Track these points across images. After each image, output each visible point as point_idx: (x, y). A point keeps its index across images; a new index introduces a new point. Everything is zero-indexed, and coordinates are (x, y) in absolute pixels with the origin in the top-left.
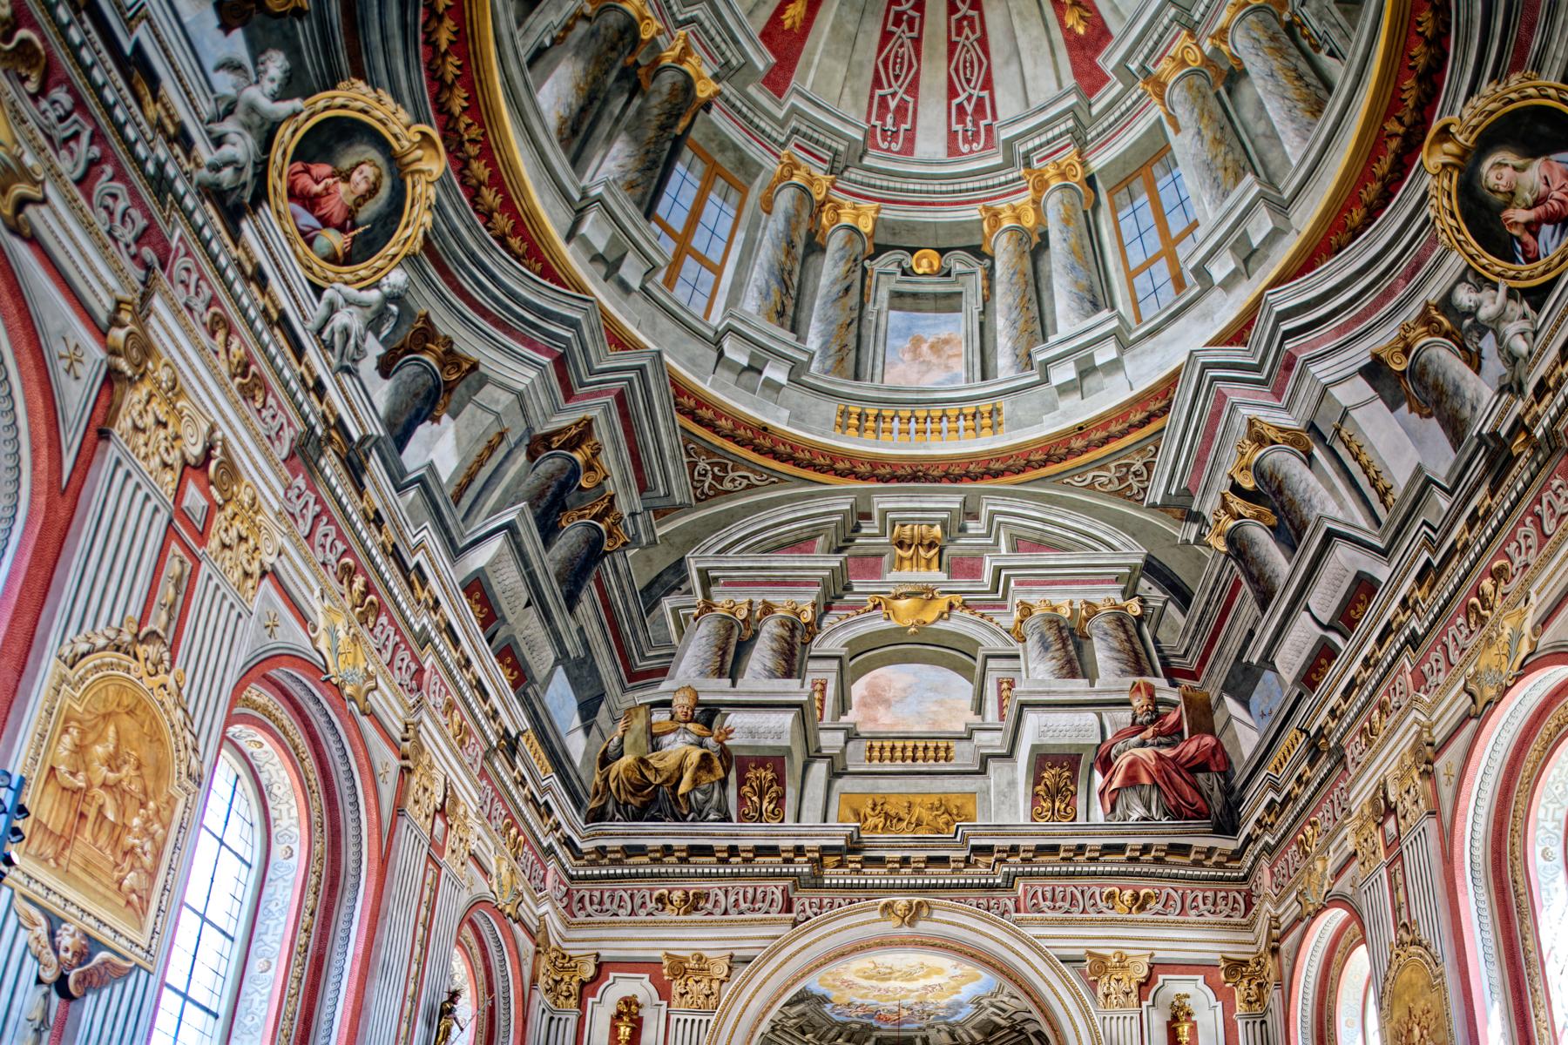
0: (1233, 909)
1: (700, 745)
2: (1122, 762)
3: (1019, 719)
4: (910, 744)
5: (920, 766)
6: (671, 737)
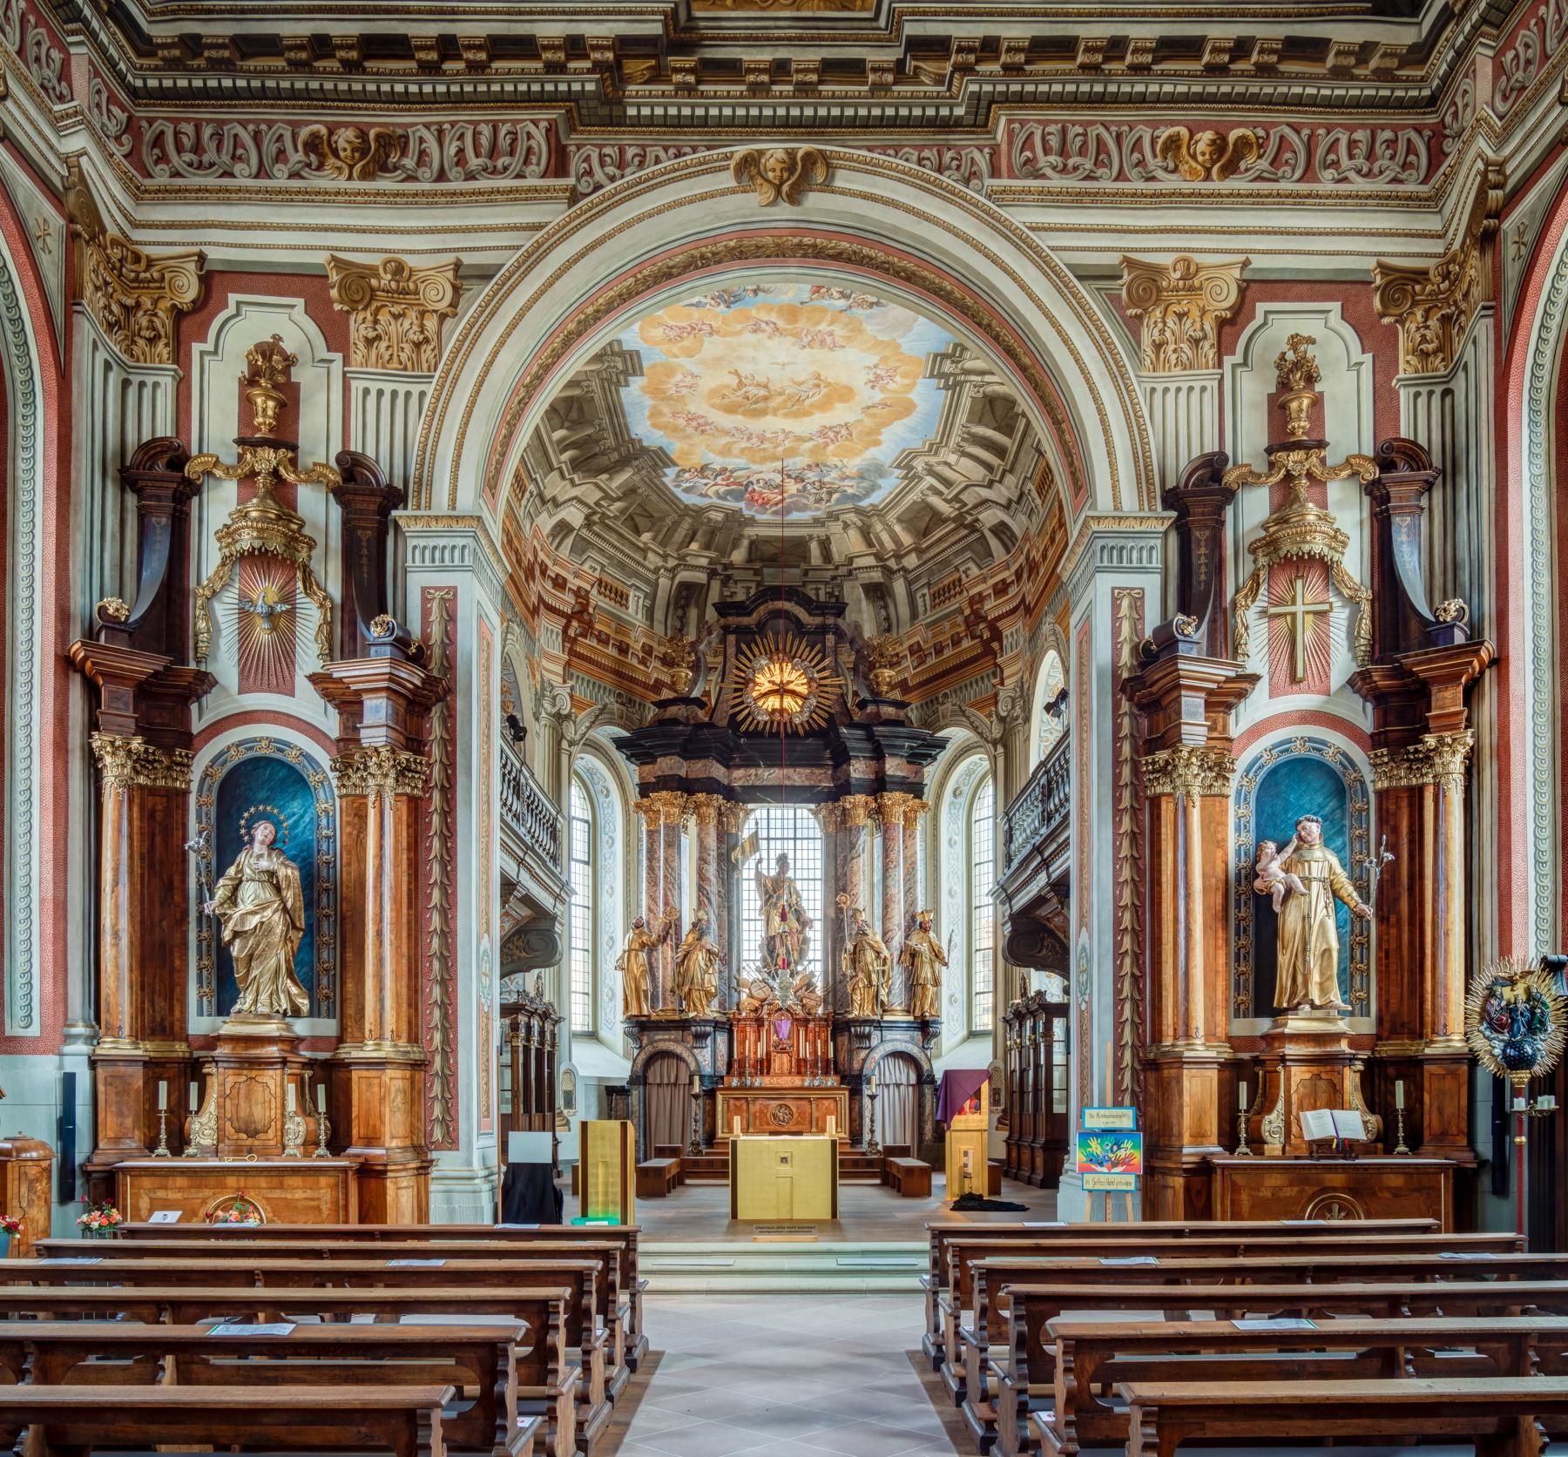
0: (1405, 166)
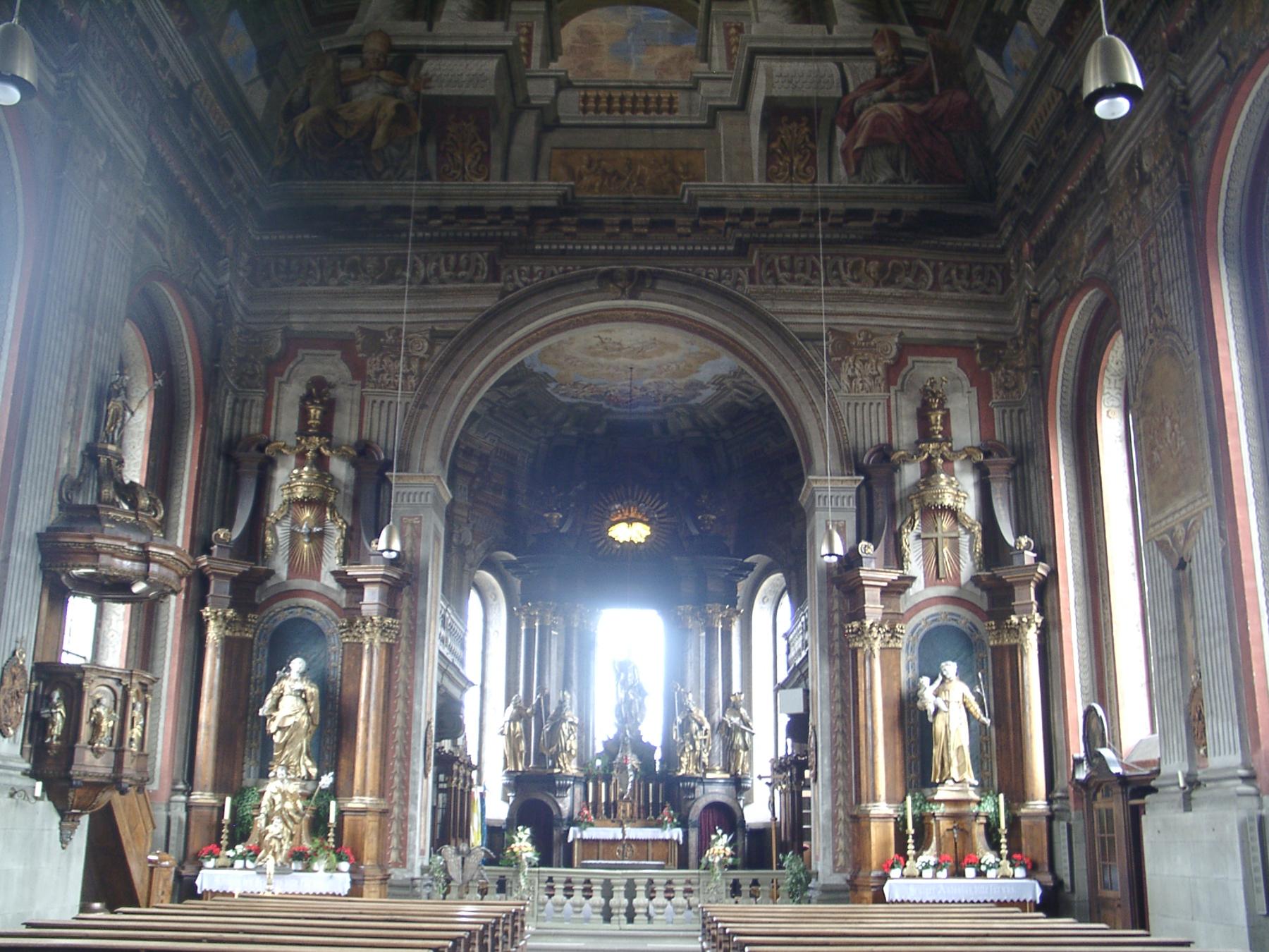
0: (990, 284)
1: (395, 95)
2: (866, 118)
3: (750, 69)
4: (630, 94)
5: (641, 119)
6: (363, 86)
